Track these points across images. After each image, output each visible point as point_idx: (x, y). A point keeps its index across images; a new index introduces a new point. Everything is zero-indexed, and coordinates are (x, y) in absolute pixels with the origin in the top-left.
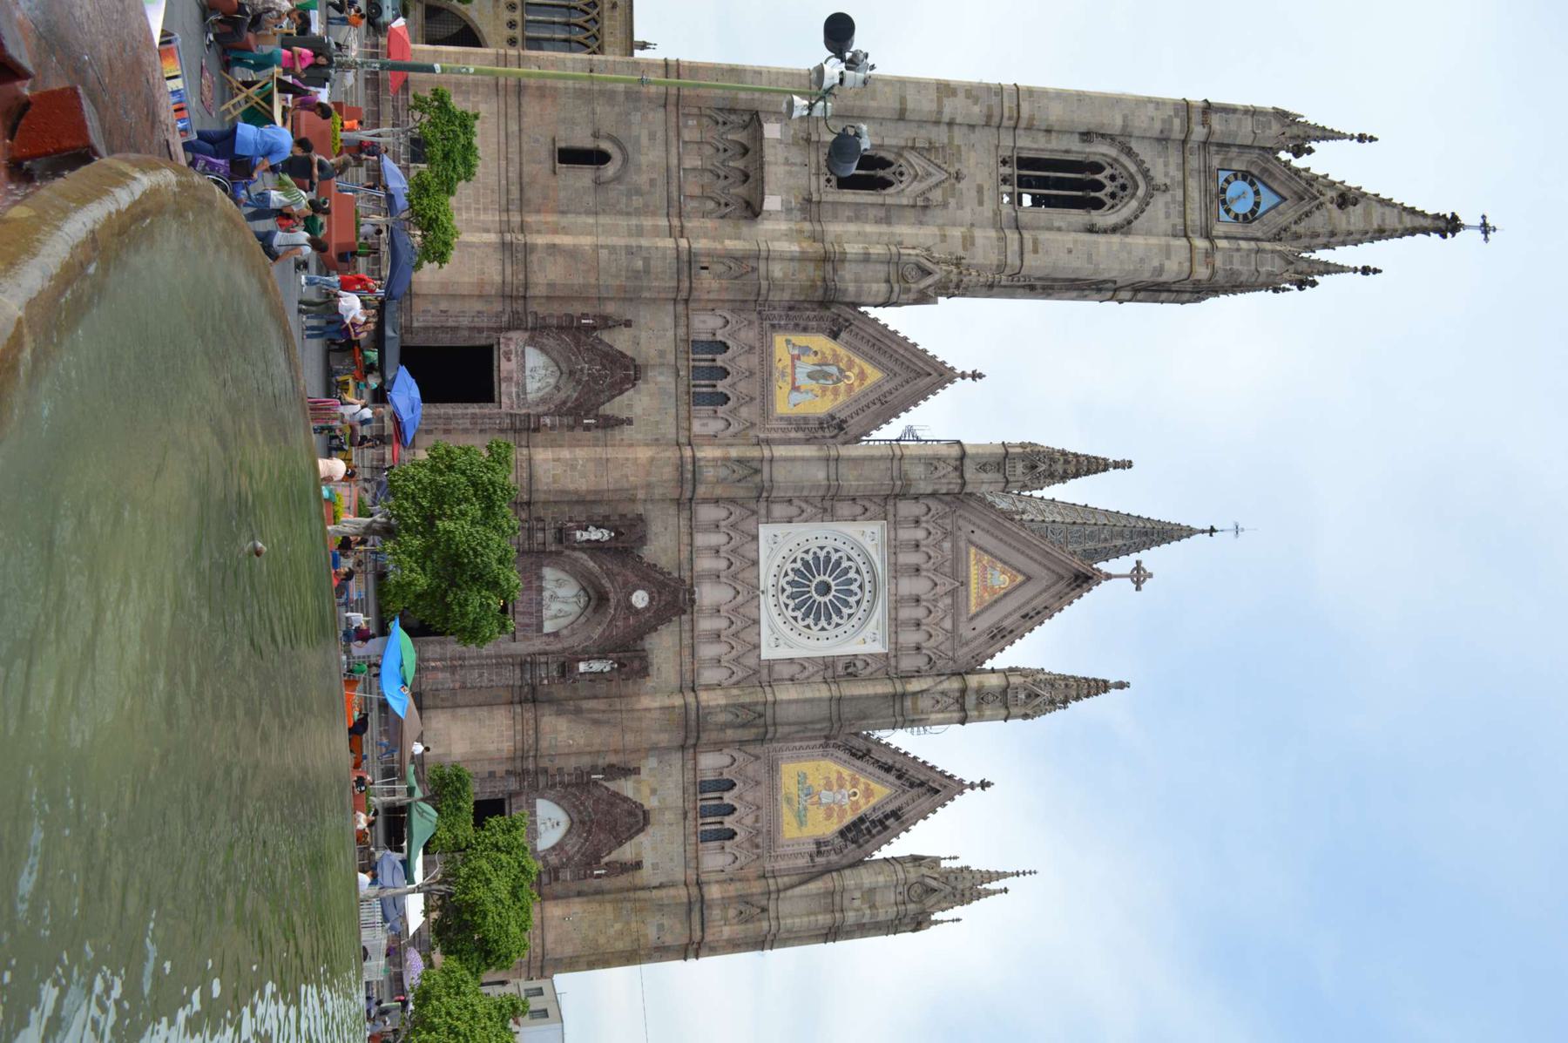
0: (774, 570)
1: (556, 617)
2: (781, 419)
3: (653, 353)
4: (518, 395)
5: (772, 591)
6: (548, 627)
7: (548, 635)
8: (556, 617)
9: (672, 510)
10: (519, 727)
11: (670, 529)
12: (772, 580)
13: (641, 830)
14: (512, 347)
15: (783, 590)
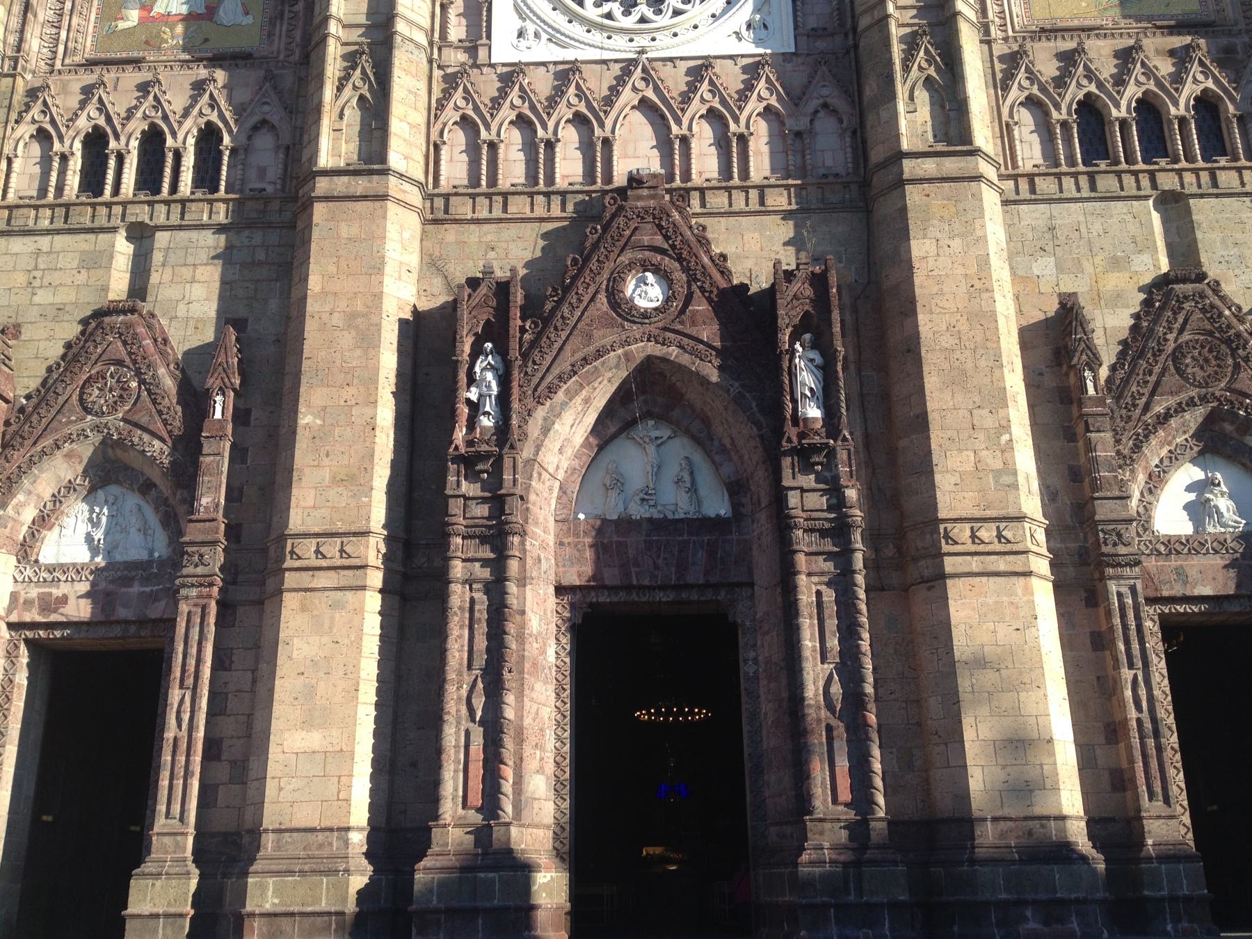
0: (597, 37)
1: (693, 489)
2: (270, 35)
3: (81, 278)
4: (145, 581)
5: (642, 41)
6: (717, 505)
7: (736, 506)
8: (693, 489)
9: (451, 234)
10: (975, 564)
11: (489, 238)
12: (620, 41)
13: (1216, 287)
14: (34, 592)
15: (643, 20)
